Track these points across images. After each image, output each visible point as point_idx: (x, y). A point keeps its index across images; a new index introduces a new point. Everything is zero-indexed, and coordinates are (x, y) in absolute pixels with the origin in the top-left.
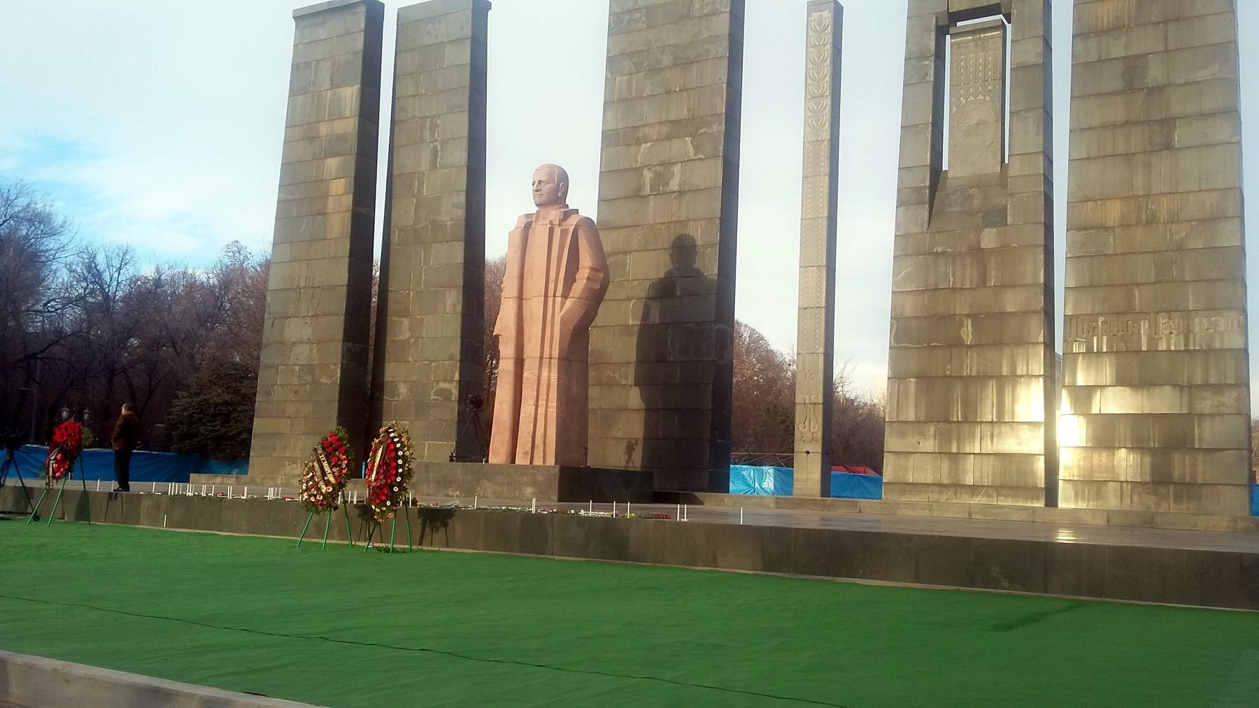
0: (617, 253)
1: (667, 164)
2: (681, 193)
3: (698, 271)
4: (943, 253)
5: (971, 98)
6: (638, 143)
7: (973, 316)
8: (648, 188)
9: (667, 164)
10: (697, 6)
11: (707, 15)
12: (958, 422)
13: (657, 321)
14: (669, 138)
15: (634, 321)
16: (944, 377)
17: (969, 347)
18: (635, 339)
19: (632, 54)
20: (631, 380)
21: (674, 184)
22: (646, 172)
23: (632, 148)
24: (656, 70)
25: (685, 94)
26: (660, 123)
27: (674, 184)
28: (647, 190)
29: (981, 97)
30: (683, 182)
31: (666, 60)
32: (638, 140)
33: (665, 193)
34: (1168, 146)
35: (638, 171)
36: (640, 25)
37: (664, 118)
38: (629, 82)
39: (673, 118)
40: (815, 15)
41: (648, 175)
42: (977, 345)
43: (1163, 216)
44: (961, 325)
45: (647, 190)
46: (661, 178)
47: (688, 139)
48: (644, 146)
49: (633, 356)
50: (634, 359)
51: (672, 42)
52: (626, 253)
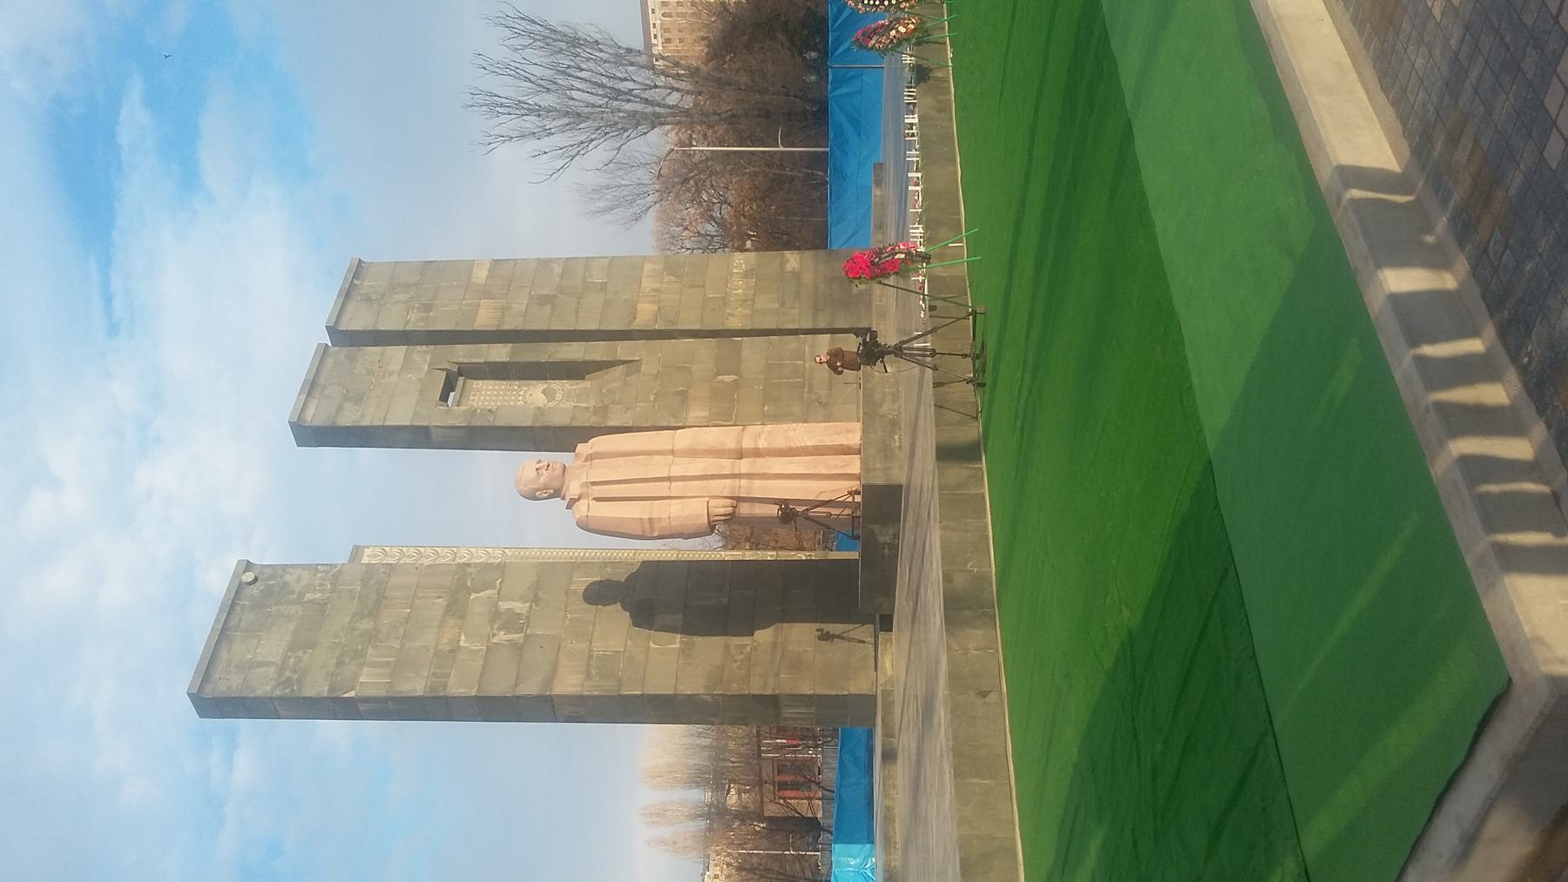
1: (495, 615)
2: (536, 600)
6: (455, 649)
7: (718, 374)
9: (495, 615)
11: (333, 585)
13: (680, 617)
14: (462, 617)
15: (676, 641)
18: (698, 639)
19: (340, 664)
20: (746, 640)
22: (495, 640)
24: (372, 638)
27: (520, 607)
28: (518, 637)
30: (523, 599)
31: (367, 625)
32: (451, 651)
33: (528, 618)
34: (603, 287)
39: (441, 612)
41: (502, 636)
43: (657, 285)
45: (518, 637)
46: (512, 622)
47: (473, 596)
49: (718, 641)
51: (347, 619)
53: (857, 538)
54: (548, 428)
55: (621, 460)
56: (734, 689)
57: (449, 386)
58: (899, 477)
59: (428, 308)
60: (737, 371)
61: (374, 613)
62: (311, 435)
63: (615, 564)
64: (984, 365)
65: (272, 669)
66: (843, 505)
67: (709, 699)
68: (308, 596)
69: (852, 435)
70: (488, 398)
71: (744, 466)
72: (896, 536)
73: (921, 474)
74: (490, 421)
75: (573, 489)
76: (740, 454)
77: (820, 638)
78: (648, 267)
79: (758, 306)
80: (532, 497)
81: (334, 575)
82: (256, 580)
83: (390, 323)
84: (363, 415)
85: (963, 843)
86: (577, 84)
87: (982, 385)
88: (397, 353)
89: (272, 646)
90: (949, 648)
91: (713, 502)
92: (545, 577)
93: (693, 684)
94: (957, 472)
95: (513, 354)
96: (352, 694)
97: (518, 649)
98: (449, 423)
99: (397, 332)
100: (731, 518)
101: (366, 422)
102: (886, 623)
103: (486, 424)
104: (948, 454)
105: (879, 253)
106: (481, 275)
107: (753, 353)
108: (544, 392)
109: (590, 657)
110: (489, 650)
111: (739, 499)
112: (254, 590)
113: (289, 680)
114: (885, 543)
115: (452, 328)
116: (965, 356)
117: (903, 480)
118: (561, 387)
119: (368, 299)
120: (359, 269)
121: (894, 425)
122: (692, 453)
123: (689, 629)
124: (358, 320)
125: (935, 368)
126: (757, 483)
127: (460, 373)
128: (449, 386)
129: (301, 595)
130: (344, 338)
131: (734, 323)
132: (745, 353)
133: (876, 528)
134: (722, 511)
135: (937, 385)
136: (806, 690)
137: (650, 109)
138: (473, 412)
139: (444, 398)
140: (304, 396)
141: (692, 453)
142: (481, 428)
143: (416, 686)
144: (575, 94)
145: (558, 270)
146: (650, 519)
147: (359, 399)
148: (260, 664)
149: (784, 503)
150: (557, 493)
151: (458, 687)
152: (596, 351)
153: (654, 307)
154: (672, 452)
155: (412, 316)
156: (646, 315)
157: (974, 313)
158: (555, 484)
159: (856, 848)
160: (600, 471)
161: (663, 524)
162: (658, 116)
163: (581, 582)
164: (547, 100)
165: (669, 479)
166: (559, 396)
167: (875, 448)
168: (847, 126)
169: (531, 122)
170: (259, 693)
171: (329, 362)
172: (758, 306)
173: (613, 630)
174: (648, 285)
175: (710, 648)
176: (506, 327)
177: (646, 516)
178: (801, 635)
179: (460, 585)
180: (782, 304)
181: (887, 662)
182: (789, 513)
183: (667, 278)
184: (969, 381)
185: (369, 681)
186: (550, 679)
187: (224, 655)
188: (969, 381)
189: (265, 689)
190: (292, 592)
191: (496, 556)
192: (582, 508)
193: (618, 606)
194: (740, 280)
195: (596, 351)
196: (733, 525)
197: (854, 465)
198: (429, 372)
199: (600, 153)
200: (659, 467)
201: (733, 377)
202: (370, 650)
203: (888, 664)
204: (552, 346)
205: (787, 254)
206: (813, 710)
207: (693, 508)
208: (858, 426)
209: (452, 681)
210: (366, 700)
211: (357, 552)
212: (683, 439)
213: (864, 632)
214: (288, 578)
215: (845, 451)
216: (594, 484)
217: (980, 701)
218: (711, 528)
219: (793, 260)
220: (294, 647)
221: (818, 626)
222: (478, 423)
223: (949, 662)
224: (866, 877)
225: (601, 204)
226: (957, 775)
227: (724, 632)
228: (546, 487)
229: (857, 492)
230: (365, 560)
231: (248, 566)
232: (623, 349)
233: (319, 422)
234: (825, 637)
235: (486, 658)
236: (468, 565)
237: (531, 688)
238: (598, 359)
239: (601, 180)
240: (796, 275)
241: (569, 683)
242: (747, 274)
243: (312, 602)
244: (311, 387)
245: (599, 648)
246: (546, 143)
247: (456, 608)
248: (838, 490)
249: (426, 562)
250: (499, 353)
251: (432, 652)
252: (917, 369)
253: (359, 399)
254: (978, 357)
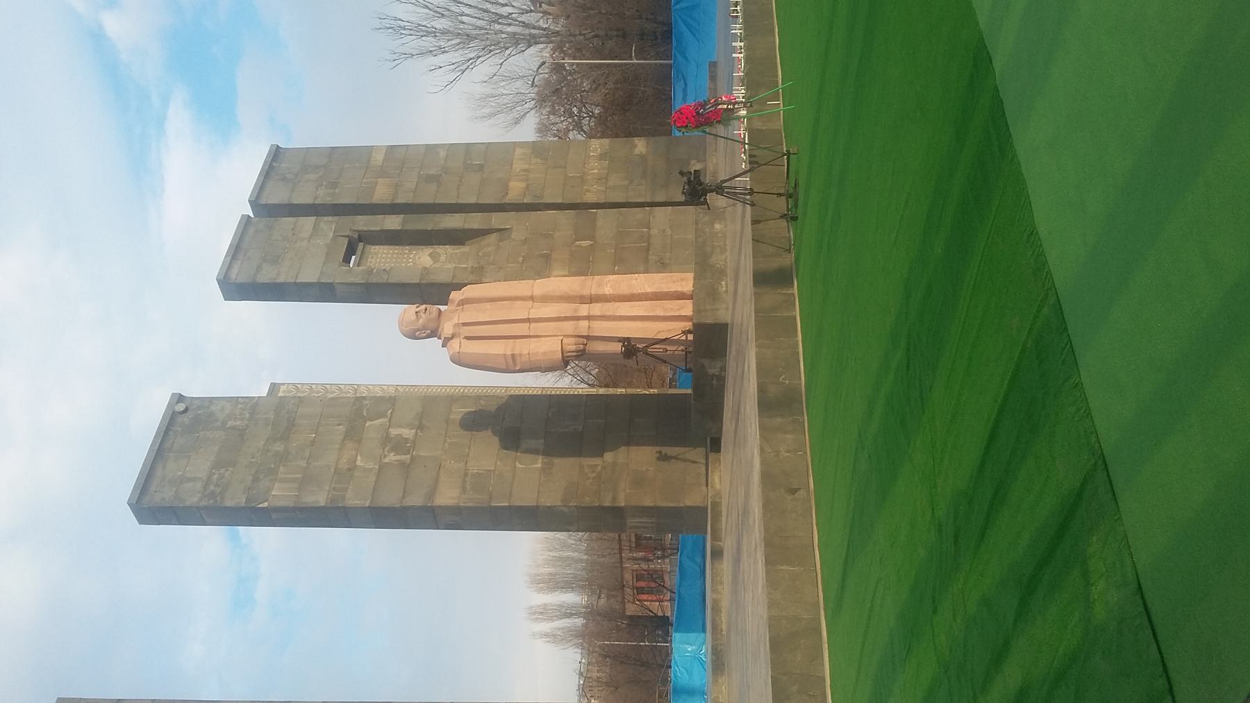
0: (464, 482)
1: (386, 439)
2: (420, 427)
3: (499, 409)
6: (352, 468)
8: (403, 457)
9: (386, 439)
10: (238, 423)
11: (251, 414)
13: (542, 441)
14: (359, 442)
15: (539, 462)
18: (557, 461)
19: (256, 479)
20: (596, 461)
22: (386, 460)
23: (357, 474)
25: (321, 429)
26: (340, 449)
27: (408, 433)
28: (406, 458)
30: (410, 426)
31: (279, 447)
32: (349, 470)
35: (382, 468)
37: (337, 446)
38: (284, 481)
39: (341, 437)
41: (392, 457)
43: (527, 166)
45: (406, 458)
46: (399, 445)
48: (358, 463)
50: (577, 459)
52: (466, 475)
53: (689, 370)
54: (432, 285)
55: (488, 305)
56: (587, 501)
57: (351, 251)
58: (723, 315)
59: (335, 185)
60: (592, 238)
61: (285, 437)
62: (238, 288)
63: (488, 397)
64: (796, 202)
65: (199, 485)
66: (677, 342)
67: (565, 509)
68: (230, 423)
69: (685, 282)
70: (384, 260)
71: (597, 309)
72: (723, 369)
73: (740, 307)
74: (384, 278)
75: (447, 329)
76: (592, 299)
77: (659, 459)
78: (519, 151)
79: (610, 183)
80: (413, 335)
81: (251, 405)
82: (186, 410)
83: (303, 197)
84: (278, 274)
85: (773, 623)
86: (467, 10)
87: (794, 219)
88: (308, 222)
89: (201, 465)
90: (762, 450)
91: (566, 341)
92: (430, 406)
93: (552, 498)
94: (772, 297)
95: (404, 222)
96: (266, 504)
97: (405, 468)
98: (351, 280)
99: (309, 205)
100: (581, 354)
101: (281, 280)
102: (715, 445)
103: (381, 281)
104: (763, 279)
105: (703, 105)
106: (378, 158)
107: (606, 222)
108: (430, 255)
109: (466, 475)
110: (380, 469)
111: (588, 338)
112: (185, 419)
113: (213, 494)
114: (713, 375)
115: (354, 202)
116: (780, 195)
117: (729, 320)
118: (444, 251)
119: (284, 179)
120: (276, 154)
121: (721, 273)
122: (546, 299)
123: (549, 451)
124: (276, 196)
125: (753, 205)
126: (605, 324)
127: (360, 239)
128: (351, 251)
129: (224, 423)
130: (268, 209)
131: (591, 198)
132: (600, 223)
133: (706, 362)
134: (573, 348)
135: (755, 222)
136: (648, 502)
137: (527, 31)
138: (370, 272)
139: (347, 260)
141: (546, 299)
142: (377, 284)
143: (319, 498)
144: (465, 19)
145: (442, 154)
146: (513, 356)
147: (275, 261)
148: (189, 480)
149: (626, 341)
150: (434, 334)
151: (353, 499)
152: (475, 221)
153: (524, 185)
154: (532, 298)
155: (321, 192)
156: (516, 190)
157: (788, 154)
158: (432, 325)
159: (693, 636)
160: (470, 314)
161: (525, 359)
162: (533, 36)
163: (458, 412)
164: (441, 24)
165: (528, 320)
166: (443, 258)
167: (706, 292)
168: (684, 28)
169: (429, 42)
170: (188, 503)
171: (251, 230)
172: (610, 183)
173: (486, 454)
174: (518, 166)
175: (567, 469)
176: (398, 201)
177: (509, 353)
178: (641, 457)
179: (358, 412)
180: (631, 182)
181: (715, 479)
182: (630, 348)
183: (534, 161)
184: (783, 216)
185: (280, 494)
186: (433, 490)
187: (159, 472)
188: (783, 216)
189: (193, 500)
190: (217, 420)
191: (392, 390)
192: (455, 344)
193: (489, 432)
194: (595, 161)
195: (475, 221)
196: (577, 356)
197: (687, 308)
198: (335, 237)
199: (486, 67)
200: (520, 311)
201: (589, 242)
202: (281, 469)
203: (717, 480)
204: (438, 217)
205: (636, 140)
206: (654, 520)
207: (549, 347)
208: (691, 276)
209: (349, 494)
210: (277, 510)
211: (274, 387)
212: (541, 286)
213: (697, 454)
214: (213, 408)
215: (680, 296)
216: (464, 324)
217: (790, 497)
218: (565, 362)
219: (641, 145)
220: (218, 464)
221: (658, 449)
222: (374, 280)
223: (762, 463)
224: (702, 663)
225: (487, 111)
226: (769, 562)
227: (579, 454)
228: (424, 328)
229: (689, 332)
230: (281, 394)
231: (180, 398)
232: (496, 220)
233: (241, 280)
234: (663, 458)
235: (378, 476)
236: (364, 398)
237: (415, 500)
238: (475, 226)
239: (488, 90)
240: (642, 157)
241: (447, 496)
242: (602, 157)
243: (234, 428)
244: (236, 250)
245: (474, 467)
246: (441, 59)
247: (354, 433)
248: (673, 330)
249: (330, 396)
250: (393, 223)
251: (333, 470)
252: (739, 205)
253: (275, 261)
254: (790, 196)
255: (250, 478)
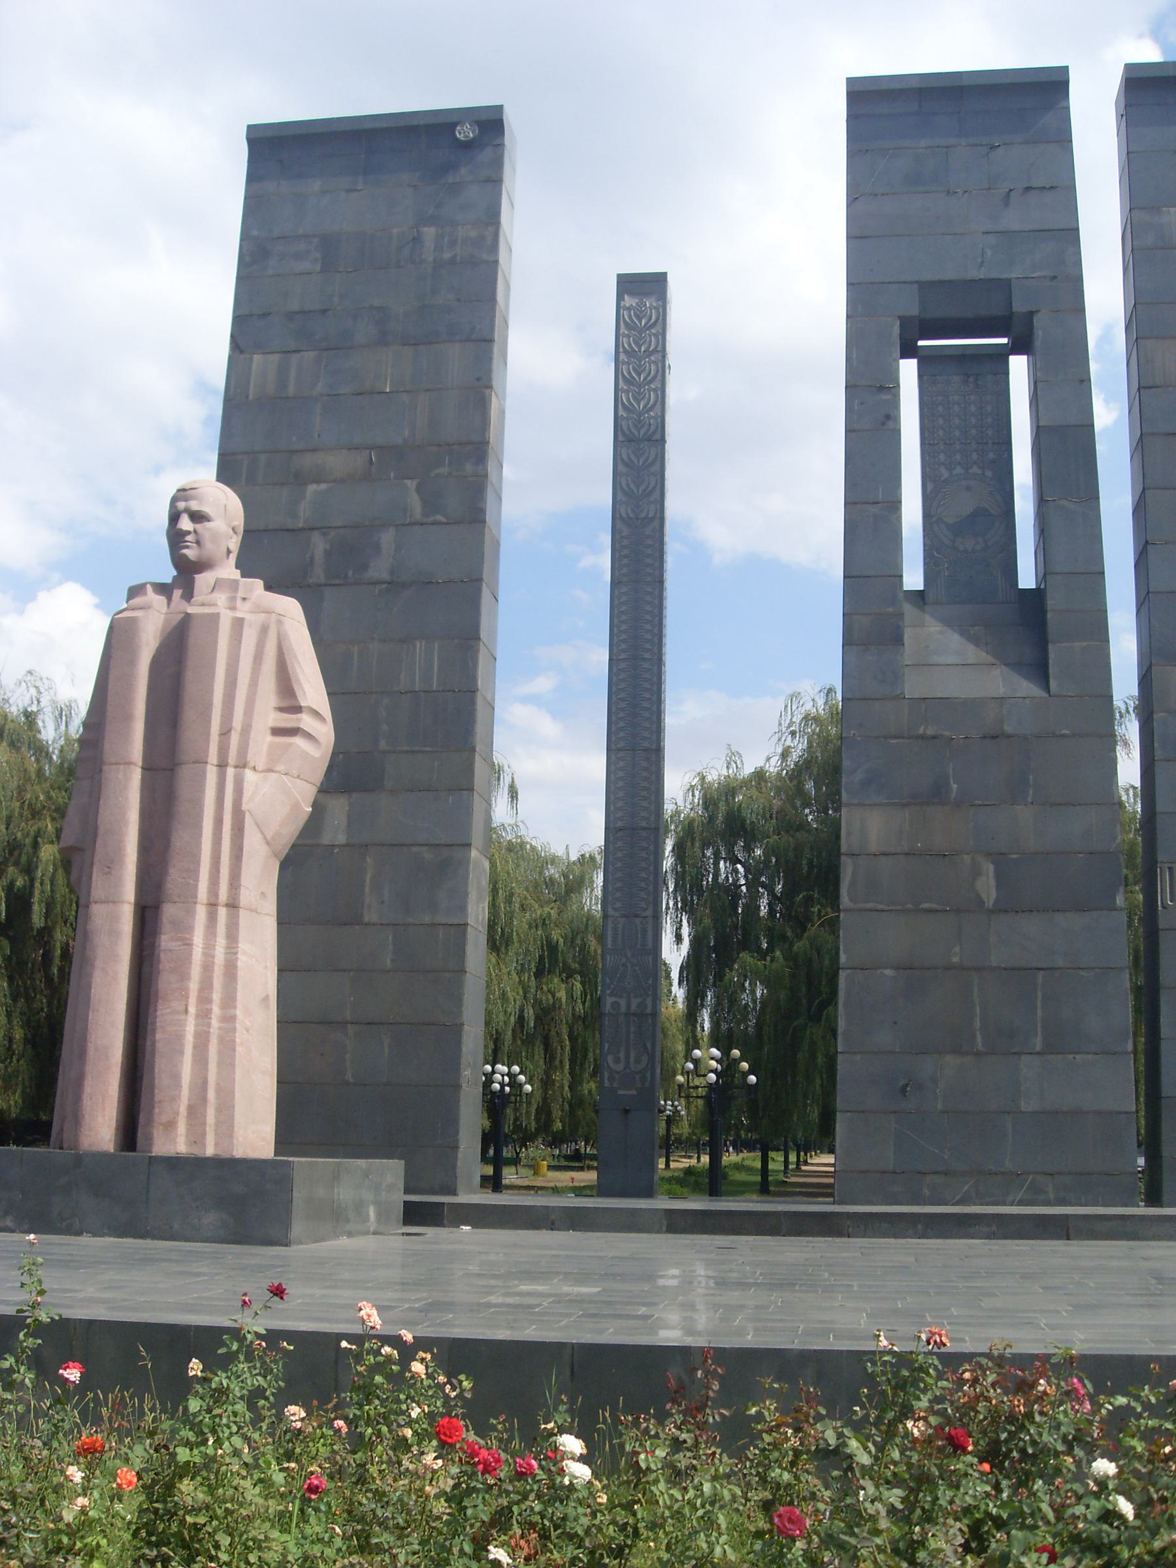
2: (394, 586)
4: (934, 737)
5: (958, 470)
6: (300, 479)
7: (999, 859)
11: (452, 261)
12: (978, 1054)
13: (342, 839)
16: (949, 967)
17: (991, 912)
19: (291, 316)
21: (379, 569)
27: (379, 569)
29: (975, 470)
36: (305, 266)
40: (629, 301)
42: (1001, 909)
44: (976, 873)
45: (318, 574)
47: (411, 484)
48: (312, 488)
60: (1010, 904)
68: (429, 232)
140: (915, 84)
255: (295, 306)
